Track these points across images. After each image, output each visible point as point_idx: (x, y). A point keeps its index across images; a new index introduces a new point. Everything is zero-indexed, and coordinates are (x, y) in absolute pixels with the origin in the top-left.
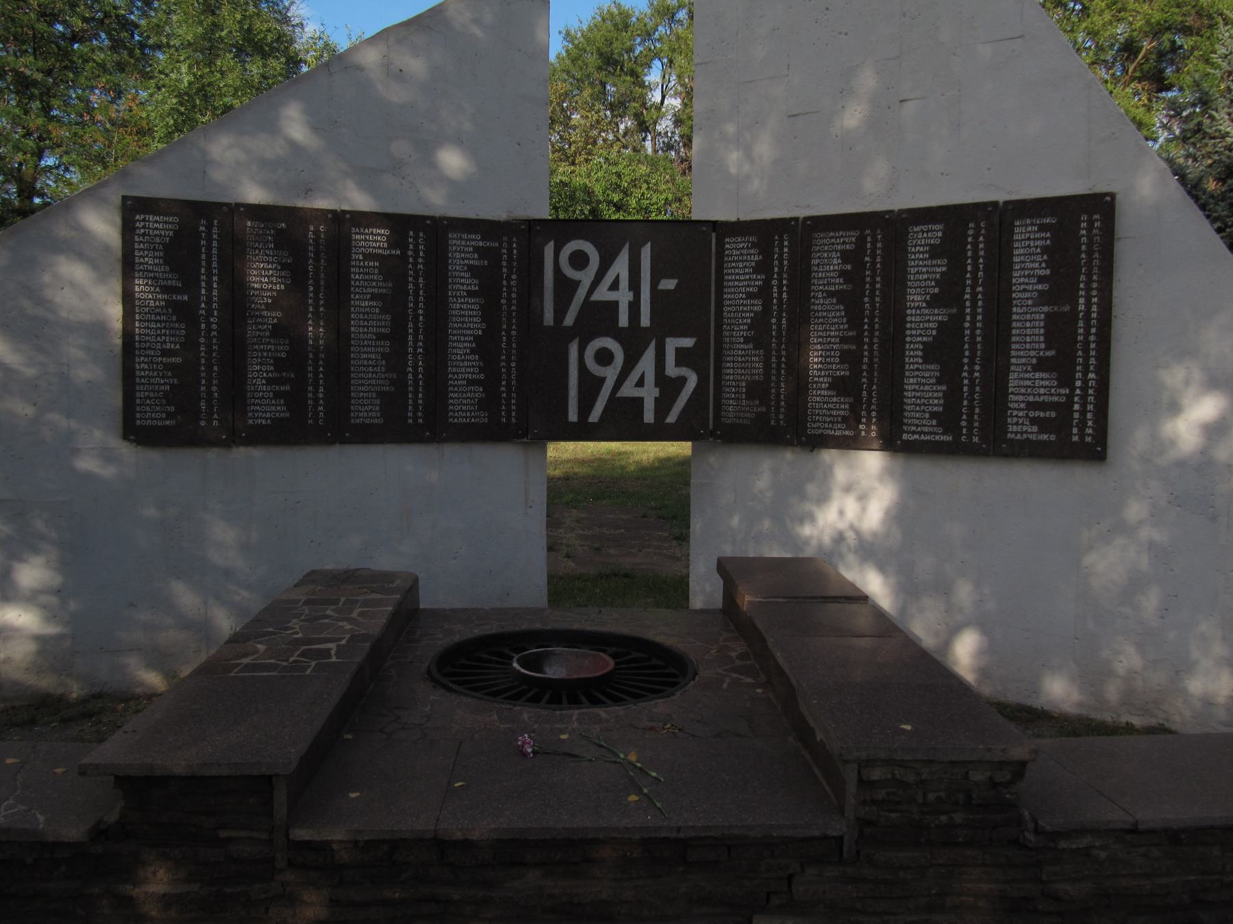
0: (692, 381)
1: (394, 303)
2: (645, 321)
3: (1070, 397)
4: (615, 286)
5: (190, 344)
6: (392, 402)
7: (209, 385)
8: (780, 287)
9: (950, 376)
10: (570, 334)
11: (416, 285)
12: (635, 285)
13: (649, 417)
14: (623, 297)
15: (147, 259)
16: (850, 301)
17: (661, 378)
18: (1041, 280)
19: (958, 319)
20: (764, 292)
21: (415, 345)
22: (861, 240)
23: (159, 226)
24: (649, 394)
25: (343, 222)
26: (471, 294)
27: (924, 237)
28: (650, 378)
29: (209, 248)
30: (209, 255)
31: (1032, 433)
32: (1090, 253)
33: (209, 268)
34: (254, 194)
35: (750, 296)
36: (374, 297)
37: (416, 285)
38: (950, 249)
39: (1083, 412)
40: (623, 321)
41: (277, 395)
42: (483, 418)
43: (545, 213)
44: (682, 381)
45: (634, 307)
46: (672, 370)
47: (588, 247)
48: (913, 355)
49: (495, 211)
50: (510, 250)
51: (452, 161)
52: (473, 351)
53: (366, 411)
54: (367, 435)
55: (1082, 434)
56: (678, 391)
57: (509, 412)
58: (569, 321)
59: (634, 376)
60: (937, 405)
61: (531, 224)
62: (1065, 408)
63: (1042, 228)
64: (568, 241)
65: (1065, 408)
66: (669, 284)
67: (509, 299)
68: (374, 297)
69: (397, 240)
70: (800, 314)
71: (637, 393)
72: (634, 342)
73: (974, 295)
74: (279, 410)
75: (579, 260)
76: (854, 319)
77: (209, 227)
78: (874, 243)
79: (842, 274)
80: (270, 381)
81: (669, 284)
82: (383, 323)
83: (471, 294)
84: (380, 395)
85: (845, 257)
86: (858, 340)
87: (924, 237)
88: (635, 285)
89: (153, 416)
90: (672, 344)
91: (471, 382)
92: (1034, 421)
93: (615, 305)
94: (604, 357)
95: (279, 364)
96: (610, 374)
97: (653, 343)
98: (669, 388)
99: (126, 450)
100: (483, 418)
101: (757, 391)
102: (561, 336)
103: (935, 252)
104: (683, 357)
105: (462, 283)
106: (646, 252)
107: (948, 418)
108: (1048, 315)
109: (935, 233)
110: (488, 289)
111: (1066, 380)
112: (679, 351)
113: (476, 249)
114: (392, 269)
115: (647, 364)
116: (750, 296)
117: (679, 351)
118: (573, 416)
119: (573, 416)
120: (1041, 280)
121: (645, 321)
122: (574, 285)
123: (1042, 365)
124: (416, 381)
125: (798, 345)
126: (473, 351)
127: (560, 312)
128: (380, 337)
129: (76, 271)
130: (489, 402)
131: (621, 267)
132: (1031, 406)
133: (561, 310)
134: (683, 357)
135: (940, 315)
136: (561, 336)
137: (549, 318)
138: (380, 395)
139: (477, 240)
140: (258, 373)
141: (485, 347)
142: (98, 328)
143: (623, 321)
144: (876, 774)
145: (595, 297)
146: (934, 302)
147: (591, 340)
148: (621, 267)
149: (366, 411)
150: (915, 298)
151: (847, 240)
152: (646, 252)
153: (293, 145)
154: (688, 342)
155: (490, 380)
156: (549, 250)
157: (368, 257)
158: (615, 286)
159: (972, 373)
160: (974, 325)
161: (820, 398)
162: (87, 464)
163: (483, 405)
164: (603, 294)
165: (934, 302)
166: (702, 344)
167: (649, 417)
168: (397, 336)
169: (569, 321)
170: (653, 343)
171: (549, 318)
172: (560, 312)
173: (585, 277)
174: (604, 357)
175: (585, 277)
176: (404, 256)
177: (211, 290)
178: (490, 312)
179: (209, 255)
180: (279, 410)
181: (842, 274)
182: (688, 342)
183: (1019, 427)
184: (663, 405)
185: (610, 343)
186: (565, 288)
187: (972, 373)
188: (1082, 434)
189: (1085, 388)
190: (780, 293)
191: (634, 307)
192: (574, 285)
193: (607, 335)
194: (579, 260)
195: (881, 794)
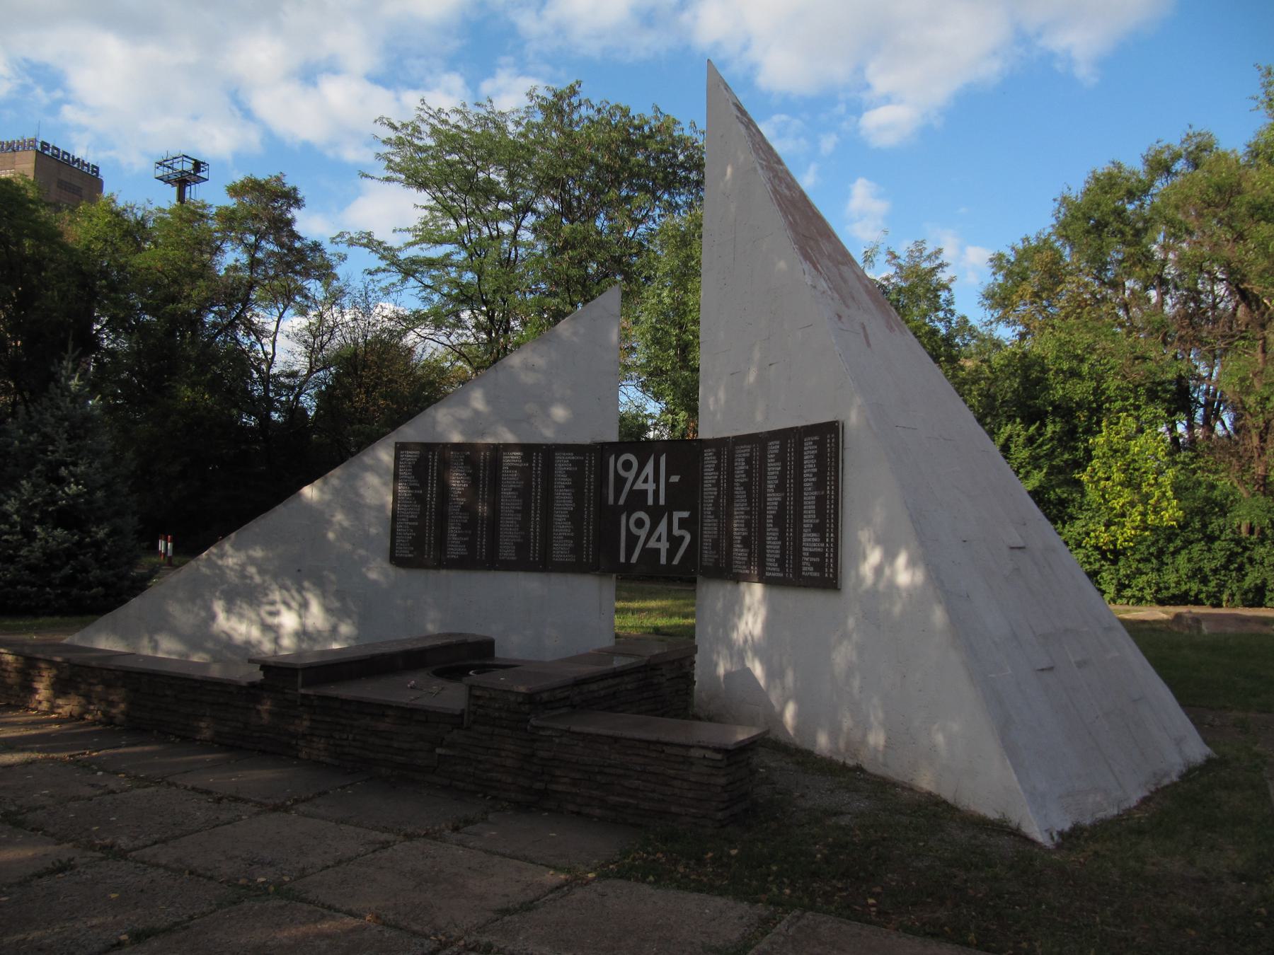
1: (524, 493)
2: (662, 502)
4: (646, 481)
5: (422, 515)
6: (522, 547)
7: (430, 537)
9: (782, 537)
11: (537, 482)
12: (656, 480)
13: (663, 561)
14: (650, 487)
15: (403, 473)
16: (747, 486)
21: (536, 517)
23: (411, 455)
24: (664, 546)
25: (498, 450)
26: (567, 487)
27: (774, 447)
28: (664, 537)
29: (433, 466)
30: (433, 470)
33: (432, 477)
34: (456, 438)
36: (514, 490)
37: (537, 482)
40: (650, 502)
41: (462, 543)
43: (613, 437)
44: (682, 538)
45: (656, 492)
46: (677, 532)
47: (632, 457)
48: (770, 521)
49: (584, 438)
50: (590, 461)
51: (559, 413)
52: (568, 520)
54: (508, 566)
56: (680, 545)
57: (588, 555)
58: (621, 502)
59: (656, 535)
62: (822, 555)
64: (622, 454)
66: (675, 479)
67: (589, 490)
68: (514, 490)
70: (731, 499)
72: (656, 514)
74: (463, 551)
75: (627, 465)
76: (749, 503)
77: (433, 456)
80: (459, 535)
81: (675, 479)
83: (567, 487)
84: (516, 544)
85: (748, 461)
87: (774, 447)
88: (656, 480)
89: (404, 552)
90: (677, 515)
91: (565, 537)
93: (646, 492)
94: (640, 523)
95: (464, 526)
96: (643, 533)
98: (675, 542)
99: (392, 571)
102: (616, 511)
104: (683, 524)
105: (562, 480)
106: (663, 459)
108: (817, 497)
111: (823, 540)
112: (681, 520)
113: (571, 461)
114: (525, 473)
115: (662, 527)
117: (681, 520)
118: (622, 560)
119: (622, 560)
121: (662, 502)
122: (625, 480)
124: (535, 537)
125: (730, 516)
126: (568, 520)
127: (617, 498)
128: (518, 511)
129: (372, 479)
130: (576, 550)
131: (649, 469)
134: (683, 524)
136: (616, 511)
138: (516, 544)
140: (453, 530)
141: (575, 517)
142: (381, 508)
143: (650, 502)
144: (478, 693)
145: (635, 487)
147: (633, 513)
148: (649, 469)
150: (771, 487)
152: (663, 459)
153: (477, 412)
154: (685, 514)
157: (511, 468)
158: (646, 481)
161: (739, 552)
162: (373, 575)
163: (573, 551)
164: (640, 485)
167: (663, 561)
168: (525, 510)
169: (621, 502)
171: (611, 500)
172: (617, 498)
173: (630, 475)
175: (630, 475)
176: (531, 467)
177: (432, 490)
178: (578, 497)
179: (433, 470)
180: (463, 551)
182: (685, 514)
183: (808, 570)
184: (671, 553)
185: (641, 515)
186: (620, 481)
187: (789, 534)
191: (656, 492)
192: (625, 480)
193: (641, 510)
195: (481, 702)
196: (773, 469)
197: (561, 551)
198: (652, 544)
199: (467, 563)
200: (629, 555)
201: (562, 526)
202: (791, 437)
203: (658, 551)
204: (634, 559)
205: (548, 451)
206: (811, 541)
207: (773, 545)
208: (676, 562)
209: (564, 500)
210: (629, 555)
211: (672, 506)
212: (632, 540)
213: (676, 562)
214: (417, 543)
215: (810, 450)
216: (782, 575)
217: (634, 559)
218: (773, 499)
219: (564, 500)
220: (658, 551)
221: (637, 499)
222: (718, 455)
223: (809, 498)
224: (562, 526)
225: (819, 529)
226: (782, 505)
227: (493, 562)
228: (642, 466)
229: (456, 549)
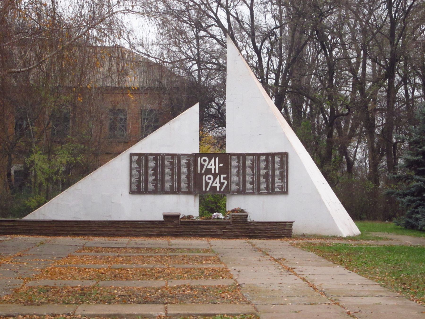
0: (226, 183)
2: (217, 172)
3: (283, 184)
4: (211, 165)
6: (172, 187)
7: (142, 184)
8: (241, 165)
9: (267, 181)
10: (202, 175)
11: (176, 166)
13: (218, 189)
14: (213, 167)
16: (252, 168)
17: (220, 182)
18: (279, 165)
19: (268, 172)
20: (238, 167)
21: (176, 177)
22: (254, 158)
23: (136, 158)
24: (218, 185)
26: (185, 167)
27: (263, 158)
28: (218, 183)
31: (278, 190)
32: (285, 161)
35: (236, 167)
37: (176, 166)
38: (267, 160)
39: (285, 186)
40: (213, 172)
41: (153, 185)
42: (187, 190)
43: (197, 152)
44: (224, 183)
45: (215, 169)
46: (222, 181)
48: (261, 177)
50: (192, 159)
53: (167, 188)
54: (167, 193)
55: (285, 190)
57: (192, 189)
58: (203, 172)
60: (265, 186)
61: (196, 154)
62: (282, 186)
63: (279, 157)
64: (203, 157)
65: (282, 186)
66: (221, 165)
67: (192, 168)
69: (173, 158)
71: (216, 185)
72: (215, 176)
73: (270, 168)
75: (205, 161)
76: (253, 172)
77: (143, 157)
78: (255, 158)
79: (251, 163)
81: (221, 165)
82: (170, 173)
83: (185, 167)
84: (170, 186)
85: (251, 161)
86: (253, 175)
89: (135, 189)
90: (222, 176)
91: (185, 183)
92: (279, 188)
94: (210, 179)
96: (211, 182)
97: (219, 176)
98: (222, 184)
100: (187, 190)
101: (237, 184)
102: (201, 175)
103: (264, 160)
104: (224, 178)
105: (184, 165)
107: (267, 188)
109: (264, 157)
110: (188, 165)
111: (282, 182)
115: (217, 180)
116: (236, 167)
118: (204, 190)
119: (204, 190)
120: (279, 165)
121: (217, 172)
122: (204, 165)
123: (279, 179)
124: (176, 183)
128: (170, 175)
130: (188, 187)
132: (278, 186)
133: (201, 169)
134: (224, 178)
135: (266, 171)
137: (199, 172)
138: (170, 186)
139: (186, 157)
141: (188, 177)
143: (213, 172)
144: (233, 217)
146: (265, 169)
149: (167, 188)
151: (251, 158)
154: (225, 176)
155: (189, 183)
156: (199, 159)
159: (270, 180)
160: (270, 173)
163: (187, 187)
164: (209, 167)
165: (265, 169)
166: (228, 176)
167: (218, 189)
168: (172, 175)
169: (203, 172)
170: (219, 176)
171: (199, 172)
174: (210, 179)
175: (206, 164)
176: (174, 161)
178: (189, 170)
181: (251, 163)
182: (225, 176)
183: (277, 189)
184: (220, 188)
186: (202, 166)
187: (270, 180)
188: (285, 190)
189: (285, 183)
190: (241, 167)
191: (215, 169)
192: (204, 165)
193: (210, 174)
194: (205, 161)
195: (234, 219)
196: (263, 164)
197: (184, 188)
198: (214, 185)
199: (155, 192)
200: (206, 188)
201: (184, 180)
202: (270, 156)
203: (216, 187)
204: (208, 190)
205: (179, 156)
206: (278, 183)
207: (263, 184)
208: (222, 190)
209: (184, 171)
210: (206, 188)
211: (220, 173)
212: (207, 184)
213: (222, 190)
214: (138, 186)
215: (277, 159)
216: (267, 191)
217: (208, 190)
218: (263, 172)
219: (184, 171)
220: (216, 187)
221: (208, 171)
222: (238, 158)
223: (277, 172)
224: (184, 180)
225: (282, 179)
226: (267, 174)
227: (163, 192)
228: (210, 161)
229: (151, 188)
